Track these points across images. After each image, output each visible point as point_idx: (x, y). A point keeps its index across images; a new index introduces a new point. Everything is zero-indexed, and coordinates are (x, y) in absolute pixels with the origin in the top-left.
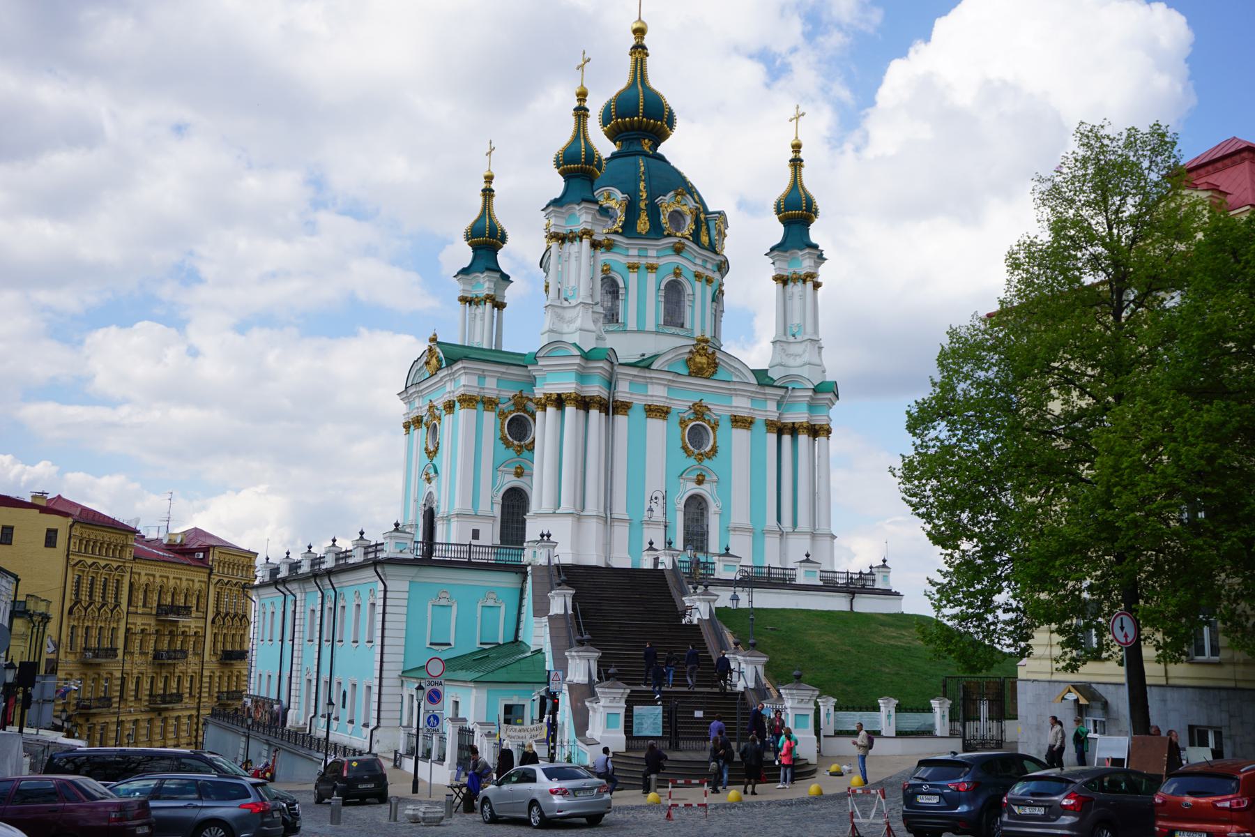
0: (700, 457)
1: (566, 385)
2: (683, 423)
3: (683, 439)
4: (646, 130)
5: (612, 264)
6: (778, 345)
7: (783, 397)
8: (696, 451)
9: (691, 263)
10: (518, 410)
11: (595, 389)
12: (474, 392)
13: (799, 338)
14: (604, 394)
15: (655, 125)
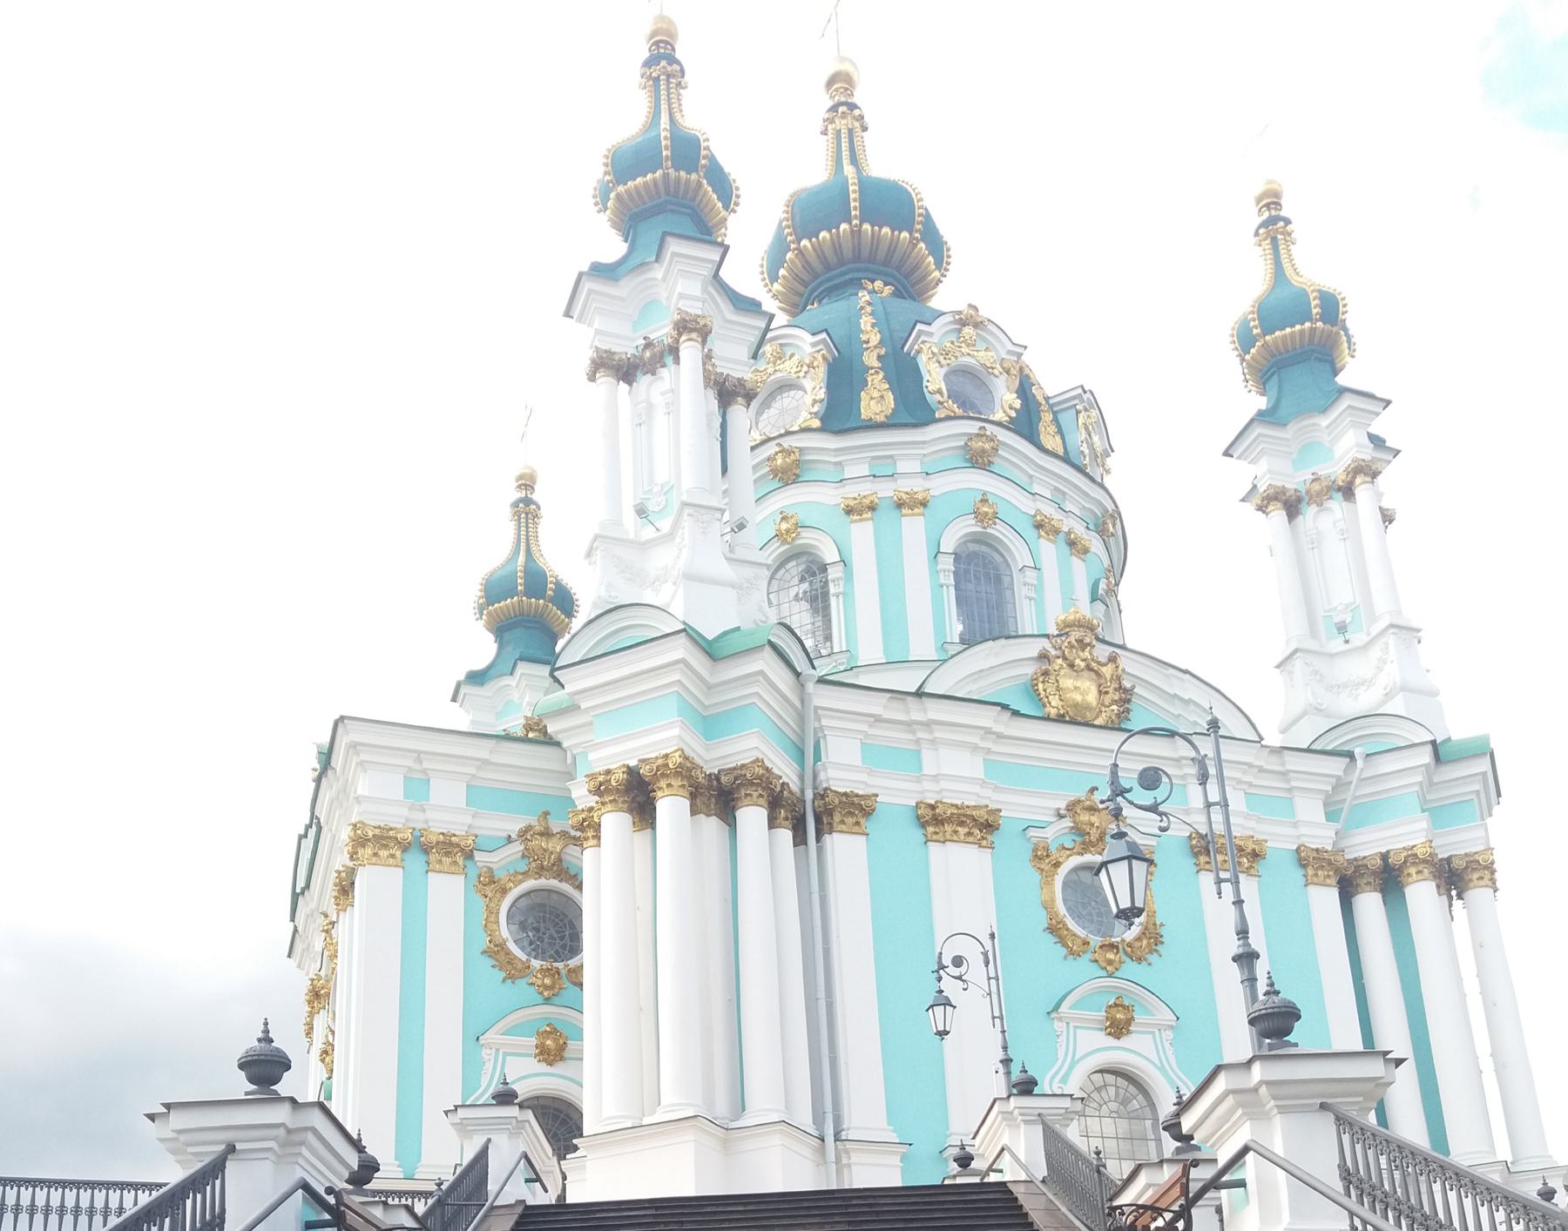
0: (1111, 955)
1: (653, 737)
2: (1043, 858)
3: (1048, 906)
4: (872, 259)
5: (802, 516)
6: (1298, 663)
7: (1340, 785)
8: (1095, 941)
9: (1022, 487)
10: (540, 871)
11: (749, 745)
12: (396, 816)
13: (1358, 638)
14: (785, 770)
15: (894, 243)
